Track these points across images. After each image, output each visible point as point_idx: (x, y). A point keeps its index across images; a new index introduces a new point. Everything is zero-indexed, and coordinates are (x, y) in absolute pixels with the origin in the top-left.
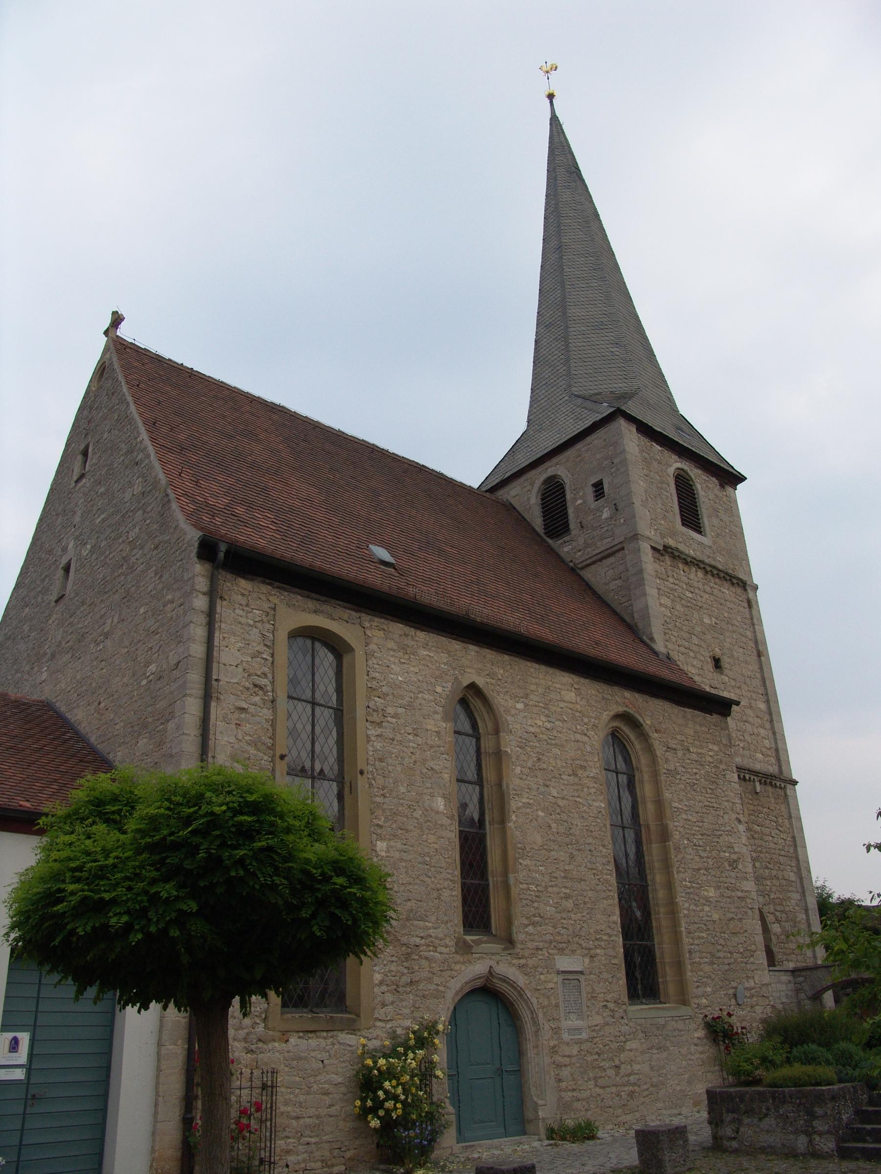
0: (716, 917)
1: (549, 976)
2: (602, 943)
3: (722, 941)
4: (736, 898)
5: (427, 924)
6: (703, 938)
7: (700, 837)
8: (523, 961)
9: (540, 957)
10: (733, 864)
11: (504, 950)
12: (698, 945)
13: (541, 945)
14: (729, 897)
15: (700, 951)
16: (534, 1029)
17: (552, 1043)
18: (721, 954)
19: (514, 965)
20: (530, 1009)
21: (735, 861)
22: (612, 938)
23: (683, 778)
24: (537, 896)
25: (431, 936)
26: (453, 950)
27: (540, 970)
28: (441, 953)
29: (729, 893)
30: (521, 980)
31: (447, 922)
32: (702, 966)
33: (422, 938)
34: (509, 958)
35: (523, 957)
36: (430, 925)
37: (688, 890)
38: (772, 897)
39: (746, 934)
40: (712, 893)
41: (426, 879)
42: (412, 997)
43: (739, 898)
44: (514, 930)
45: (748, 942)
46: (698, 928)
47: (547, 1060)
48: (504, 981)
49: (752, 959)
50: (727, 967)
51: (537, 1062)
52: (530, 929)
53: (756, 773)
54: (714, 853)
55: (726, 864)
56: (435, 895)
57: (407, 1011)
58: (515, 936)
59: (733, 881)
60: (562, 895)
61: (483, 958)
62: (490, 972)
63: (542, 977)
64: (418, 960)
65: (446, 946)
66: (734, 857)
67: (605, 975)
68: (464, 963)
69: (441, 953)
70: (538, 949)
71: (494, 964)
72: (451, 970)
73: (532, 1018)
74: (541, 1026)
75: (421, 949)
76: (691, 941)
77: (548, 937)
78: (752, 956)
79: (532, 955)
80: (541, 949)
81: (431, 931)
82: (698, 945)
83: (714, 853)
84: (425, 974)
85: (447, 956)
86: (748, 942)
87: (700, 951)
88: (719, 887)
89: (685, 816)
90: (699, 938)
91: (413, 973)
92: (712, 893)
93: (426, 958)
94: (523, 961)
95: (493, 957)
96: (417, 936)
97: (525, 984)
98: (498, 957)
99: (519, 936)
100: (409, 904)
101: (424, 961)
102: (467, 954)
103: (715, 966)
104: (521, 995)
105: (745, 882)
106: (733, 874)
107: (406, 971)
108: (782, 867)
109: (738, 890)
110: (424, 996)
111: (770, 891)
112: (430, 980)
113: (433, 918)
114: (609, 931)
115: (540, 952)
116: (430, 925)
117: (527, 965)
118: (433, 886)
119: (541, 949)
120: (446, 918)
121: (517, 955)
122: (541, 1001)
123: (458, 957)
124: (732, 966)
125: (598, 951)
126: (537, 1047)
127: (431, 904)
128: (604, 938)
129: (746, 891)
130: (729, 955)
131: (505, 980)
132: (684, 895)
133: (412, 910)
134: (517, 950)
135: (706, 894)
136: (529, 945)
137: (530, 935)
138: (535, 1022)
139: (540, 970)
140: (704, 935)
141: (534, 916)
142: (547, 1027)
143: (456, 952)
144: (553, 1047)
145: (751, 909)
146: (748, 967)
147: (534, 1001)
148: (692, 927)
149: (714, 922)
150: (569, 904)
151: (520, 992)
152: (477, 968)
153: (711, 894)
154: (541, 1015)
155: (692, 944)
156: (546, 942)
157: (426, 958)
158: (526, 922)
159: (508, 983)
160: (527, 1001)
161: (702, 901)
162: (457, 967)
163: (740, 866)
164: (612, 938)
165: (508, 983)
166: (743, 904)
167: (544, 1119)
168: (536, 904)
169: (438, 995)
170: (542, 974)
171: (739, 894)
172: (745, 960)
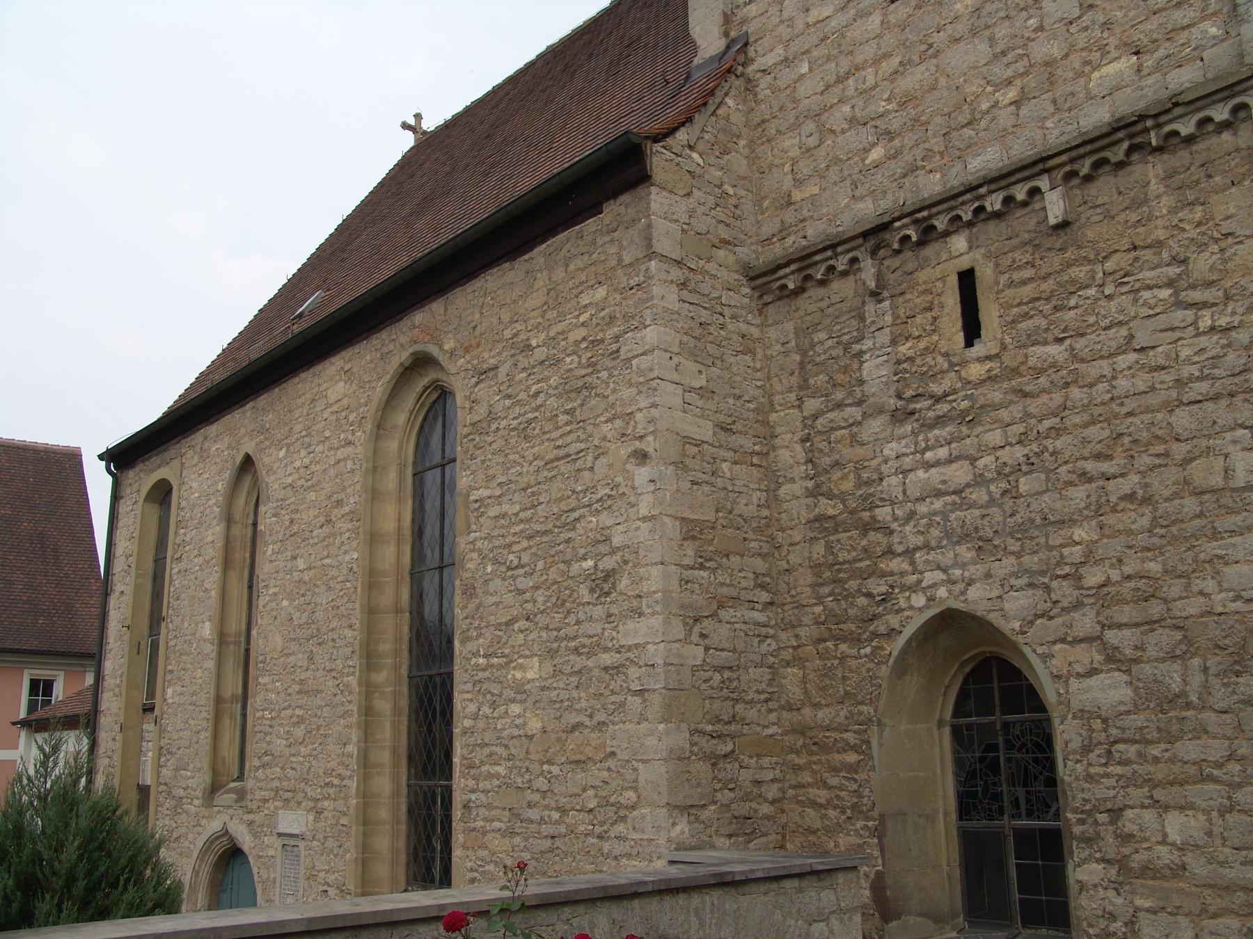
0: (534, 725)
2: (332, 791)
3: (541, 783)
4: (596, 672)
6: (497, 776)
7: (525, 544)
10: (603, 583)
12: (485, 792)
14: (579, 672)
15: (490, 807)
18: (534, 814)
21: (609, 575)
22: (344, 783)
23: (504, 423)
29: (579, 662)
32: (489, 836)
37: (481, 675)
38: (1093, 577)
39: (611, 763)
40: (533, 670)
43: (606, 669)
45: (614, 784)
46: (491, 755)
49: (620, 828)
50: (547, 843)
53: (1039, 165)
54: (553, 574)
55: (584, 593)
59: (596, 628)
60: (295, 719)
66: (608, 563)
67: (330, 843)
76: (471, 783)
77: (276, 784)
78: (623, 819)
82: (485, 792)
83: (553, 574)
86: (614, 784)
87: (490, 807)
88: (552, 653)
89: (493, 512)
90: (490, 776)
92: (533, 670)
98: (231, 811)
103: (518, 840)
105: (631, 625)
106: (598, 611)
108: (1179, 450)
109: (606, 649)
111: (1089, 558)
114: (341, 770)
124: (558, 843)
125: (326, 803)
128: (336, 781)
129: (630, 648)
130: (556, 815)
132: (469, 686)
135: (519, 675)
140: (501, 770)
145: (640, 692)
146: (606, 847)
148: (480, 754)
149: (531, 738)
150: (299, 732)
152: (215, 826)
153: (530, 675)
155: (473, 791)
161: (509, 693)
163: (624, 583)
164: (344, 783)
166: (619, 680)
171: (607, 659)
172: (598, 829)
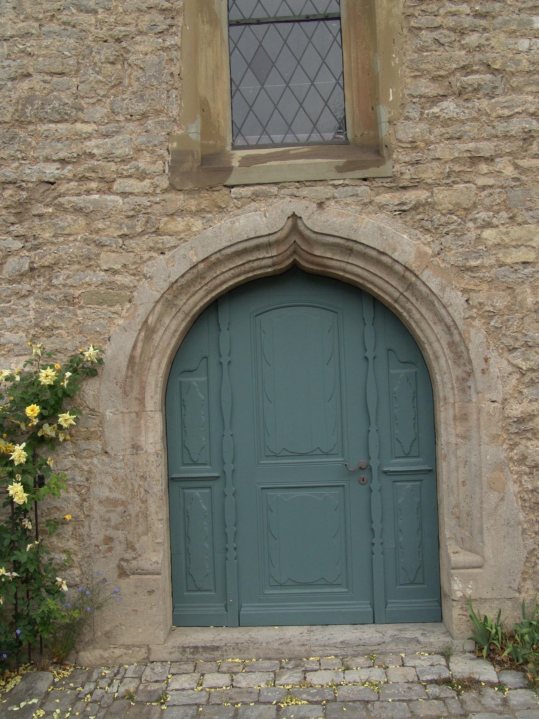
1: (516, 232)
5: (79, 126)
8: (412, 196)
9: (481, 181)
11: (340, 169)
13: (487, 148)
16: (458, 372)
17: (516, 409)
19: (382, 207)
20: (441, 320)
24: (477, 15)
25: (92, 156)
26: (165, 183)
27: (483, 215)
28: (124, 194)
30: (406, 245)
31: (144, 116)
33: (63, 162)
34: (363, 189)
35: (416, 184)
36: (89, 128)
41: (83, 17)
42: (33, 305)
44: (384, 114)
47: (493, 453)
48: (350, 251)
51: (472, 456)
52: (450, 107)
56: (109, 51)
57: (19, 337)
58: (385, 129)
61: (267, 196)
62: (295, 229)
63: (488, 233)
64: (51, 216)
65: (142, 176)
68: (199, 212)
69: (124, 194)
70: (475, 159)
71: (304, 208)
72: (157, 232)
73: (452, 345)
74: (478, 364)
75: (63, 188)
77: (516, 126)
79: (450, 179)
80: (490, 160)
81: (93, 142)
84: (73, 248)
85: (145, 201)
91: (36, 248)
93: (78, 210)
94: (412, 196)
95: (305, 191)
96: (47, 160)
97: (421, 255)
98: (322, 191)
99: (403, 130)
100: (25, 85)
101: (69, 218)
102: (211, 188)
104: (410, 286)
107: (18, 244)
110: (70, 300)
112: (88, 262)
113: (100, 112)
115: (484, 167)
116: (89, 128)
117: (432, 205)
118: (102, 33)
119: (490, 160)
120: (141, 107)
121: (393, 178)
122: (476, 299)
123: (178, 200)
126: (464, 418)
127: (92, 77)
131: (349, 247)
133: (29, 100)
134: (387, 169)
136: (442, 150)
137: (447, 122)
138: (459, 353)
139: (483, 215)
141: (466, 69)
142: (499, 365)
143: (172, 188)
144: (520, 421)
147: (455, 299)
151: (407, 276)
154: (476, 337)
156: (506, 137)
157: (78, 210)
158: (427, 88)
159: (364, 256)
160: (429, 300)
162: (179, 224)
165: (364, 256)
167: (468, 601)
168: (473, 39)
169: (111, 296)
170: (489, 225)
